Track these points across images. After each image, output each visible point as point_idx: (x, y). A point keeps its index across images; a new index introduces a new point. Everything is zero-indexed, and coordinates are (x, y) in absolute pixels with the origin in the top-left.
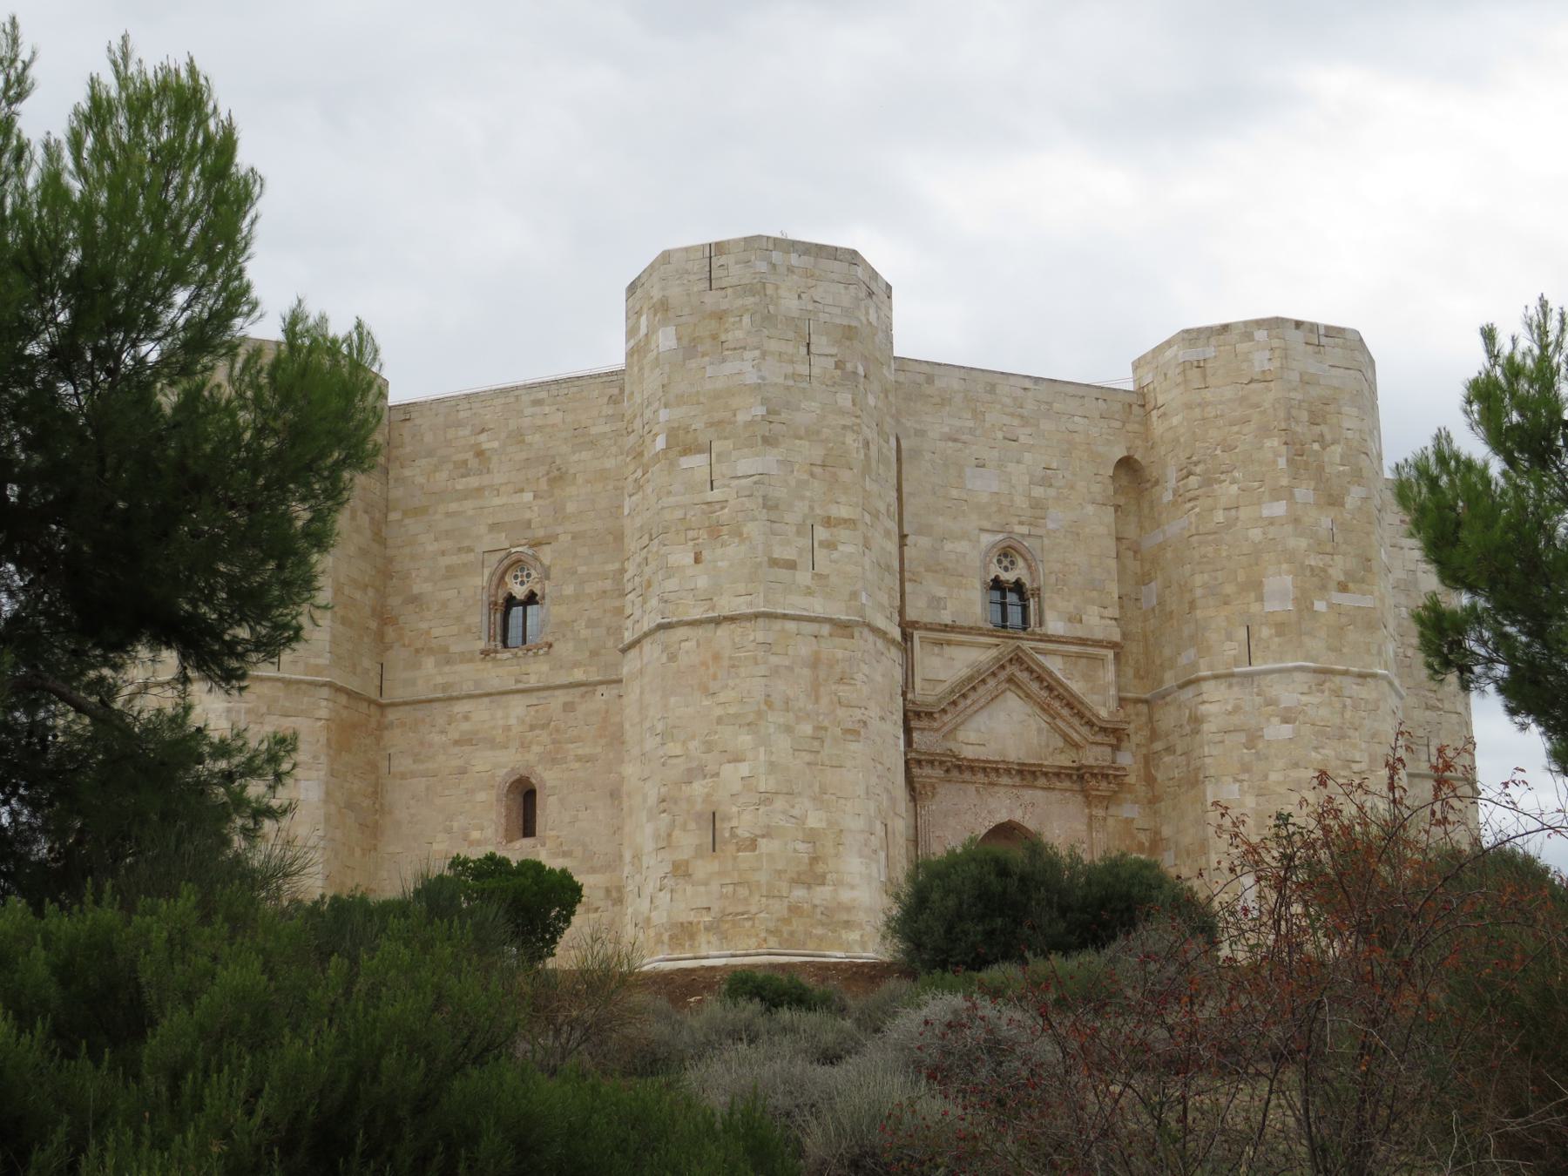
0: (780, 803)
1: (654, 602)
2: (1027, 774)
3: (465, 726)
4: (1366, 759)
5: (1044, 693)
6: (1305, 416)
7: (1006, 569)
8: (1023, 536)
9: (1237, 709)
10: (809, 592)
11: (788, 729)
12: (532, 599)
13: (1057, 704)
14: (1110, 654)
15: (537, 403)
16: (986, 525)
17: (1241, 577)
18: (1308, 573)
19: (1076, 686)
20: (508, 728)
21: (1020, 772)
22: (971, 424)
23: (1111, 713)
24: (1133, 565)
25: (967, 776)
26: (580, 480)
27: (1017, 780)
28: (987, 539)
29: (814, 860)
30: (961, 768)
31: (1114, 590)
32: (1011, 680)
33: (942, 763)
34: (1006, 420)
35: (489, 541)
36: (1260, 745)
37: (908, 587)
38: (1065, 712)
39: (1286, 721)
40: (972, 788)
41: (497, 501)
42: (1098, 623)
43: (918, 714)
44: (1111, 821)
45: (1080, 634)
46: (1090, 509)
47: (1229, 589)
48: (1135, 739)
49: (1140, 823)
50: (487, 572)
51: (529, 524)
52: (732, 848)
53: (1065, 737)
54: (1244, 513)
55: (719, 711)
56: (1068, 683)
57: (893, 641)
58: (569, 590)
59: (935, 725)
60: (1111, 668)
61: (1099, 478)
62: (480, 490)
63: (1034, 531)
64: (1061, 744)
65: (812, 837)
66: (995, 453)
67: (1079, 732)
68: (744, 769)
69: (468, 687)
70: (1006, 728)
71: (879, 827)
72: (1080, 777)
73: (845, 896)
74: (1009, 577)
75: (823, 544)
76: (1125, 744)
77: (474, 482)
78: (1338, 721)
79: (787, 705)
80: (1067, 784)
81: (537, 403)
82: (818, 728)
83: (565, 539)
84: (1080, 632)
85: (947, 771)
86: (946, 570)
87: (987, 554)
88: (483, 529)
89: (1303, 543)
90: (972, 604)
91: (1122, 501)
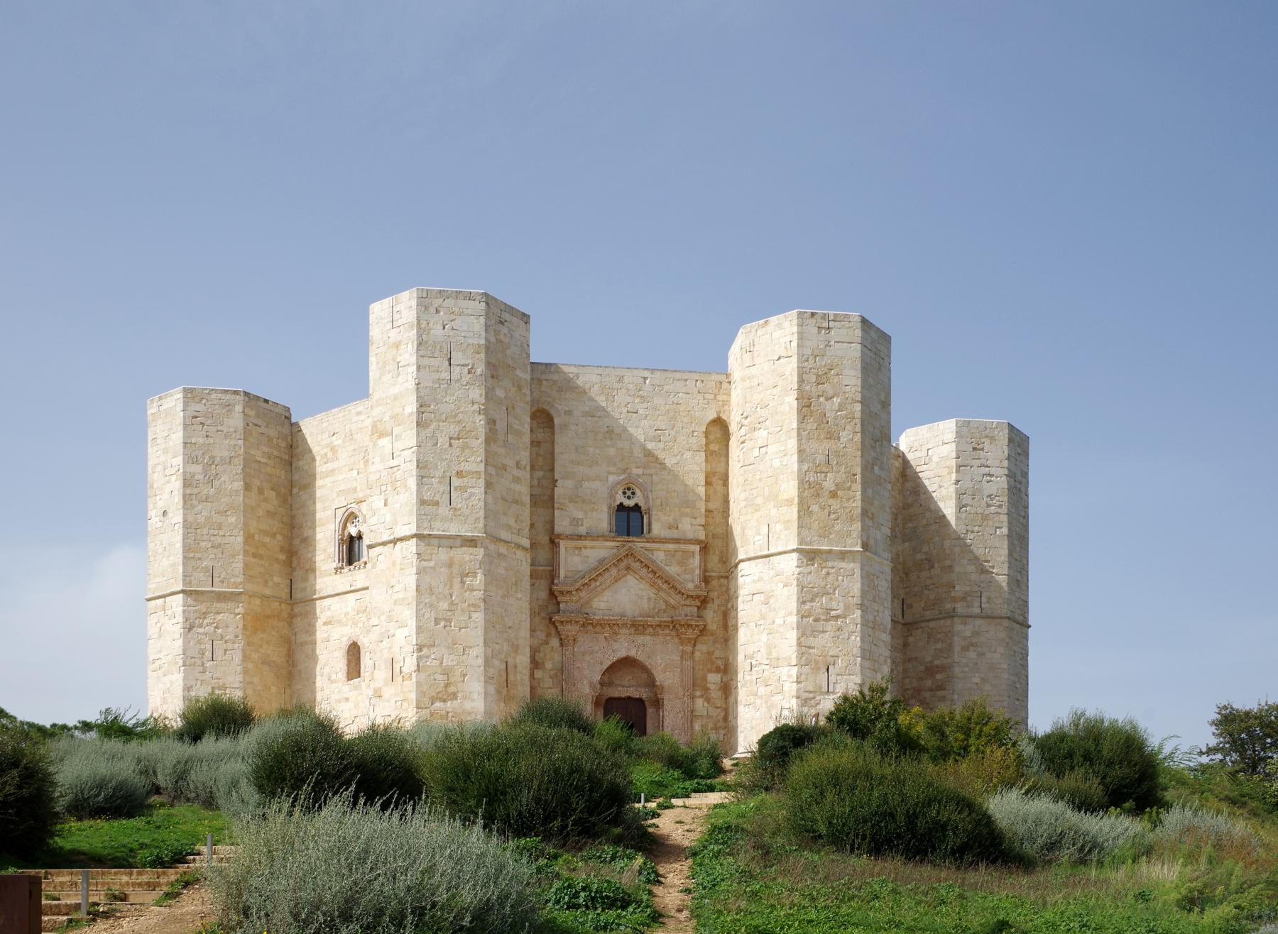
0: (425, 651)
2: (638, 626)
4: (841, 605)
5: (651, 575)
7: (629, 498)
8: (639, 476)
9: (760, 579)
11: (431, 606)
13: (659, 582)
14: (697, 548)
16: (612, 469)
17: (767, 493)
18: (806, 486)
19: (673, 570)
21: (633, 625)
23: (696, 587)
24: (720, 488)
25: (598, 629)
27: (632, 630)
28: (612, 479)
29: (447, 686)
30: (589, 624)
31: (702, 506)
32: (628, 568)
33: (577, 622)
36: (772, 601)
38: (665, 586)
39: (785, 586)
40: (601, 637)
41: (341, 477)
42: (691, 527)
43: (562, 593)
44: (697, 654)
45: (676, 536)
46: (688, 455)
47: (759, 501)
48: (717, 602)
49: (717, 654)
50: (338, 520)
52: (400, 679)
53: (666, 602)
54: (771, 449)
55: (395, 597)
56: (667, 568)
57: (518, 546)
60: (697, 557)
62: (333, 470)
63: (646, 472)
65: (447, 672)
67: (674, 599)
68: (405, 632)
70: (627, 596)
71: (497, 662)
72: (674, 625)
73: (468, 705)
74: (630, 503)
75: (462, 489)
76: (709, 605)
78: (823, 584)
79: (431, 591)
80: (667, 631)
82: (452, 603)
84: (675, 534)
85: (583, 625)
86: (584, 501)
87: (612, 488)
88: (335, 495)
90: (602, 519)
91: (714, 447)
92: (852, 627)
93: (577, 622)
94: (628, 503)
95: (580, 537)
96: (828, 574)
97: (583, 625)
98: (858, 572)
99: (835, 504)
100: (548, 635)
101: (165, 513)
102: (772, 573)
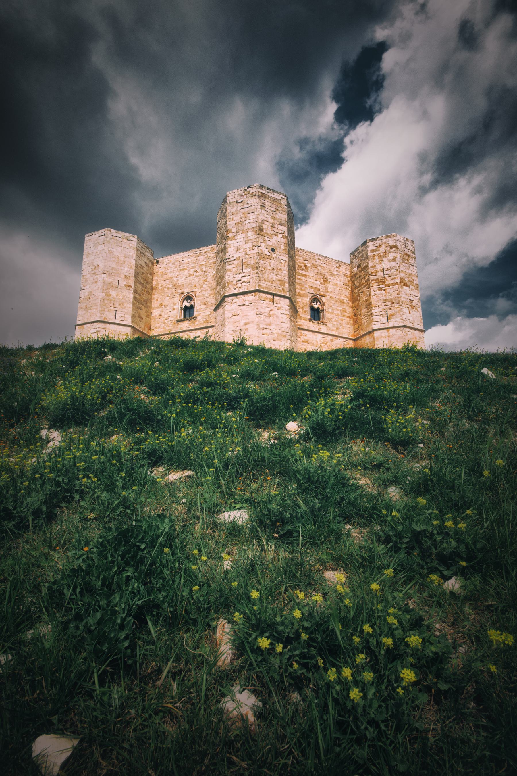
1: (398, 320)
3: (306, 338)
12: (318, 308)
15: (319, 259)
20: (317, 342)
26: (331, 283)
35: (309, 290)
50: (309, 298)
51: (319, 290)
58: (330, 310)
69: (306, 327)
77: (304, 273)
81: (319, 259)
83: (328, 297)
88: (307, 287)
101: (273, 250)
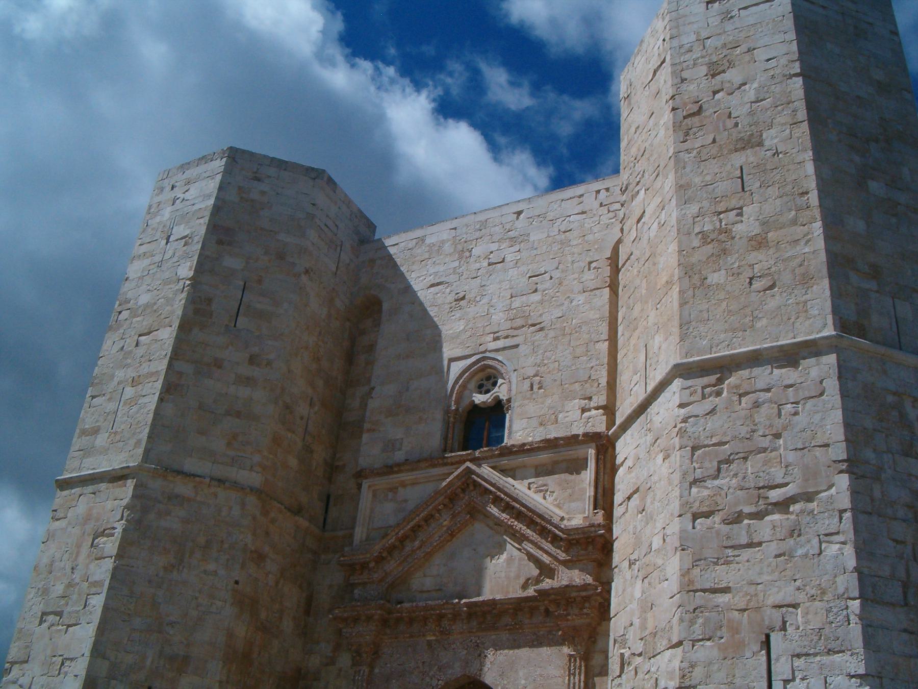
6: (704, 70)
7: (487, 392)
8: (497, 350)
10: (105, 451)
18: (696, 242)
22: (456, 264)
34: (494, 247)
37: (365, 437)
45: (551, 436)
46: (581, 298)
59: (376, 576)
61: (593, 265)
64: (536, 572)
66: (478, 280)
78: (744, 431)
84: (554, 433)
89: (694, 209)
92: (830, 523)
93: (369, 618)
94: (479, 398)
95: (389, 469)
96: (757, 405)
97: (385, 622)
98: (832, 385)
99: (762, 260)
100: (337, 648)
102: (650, 438)
